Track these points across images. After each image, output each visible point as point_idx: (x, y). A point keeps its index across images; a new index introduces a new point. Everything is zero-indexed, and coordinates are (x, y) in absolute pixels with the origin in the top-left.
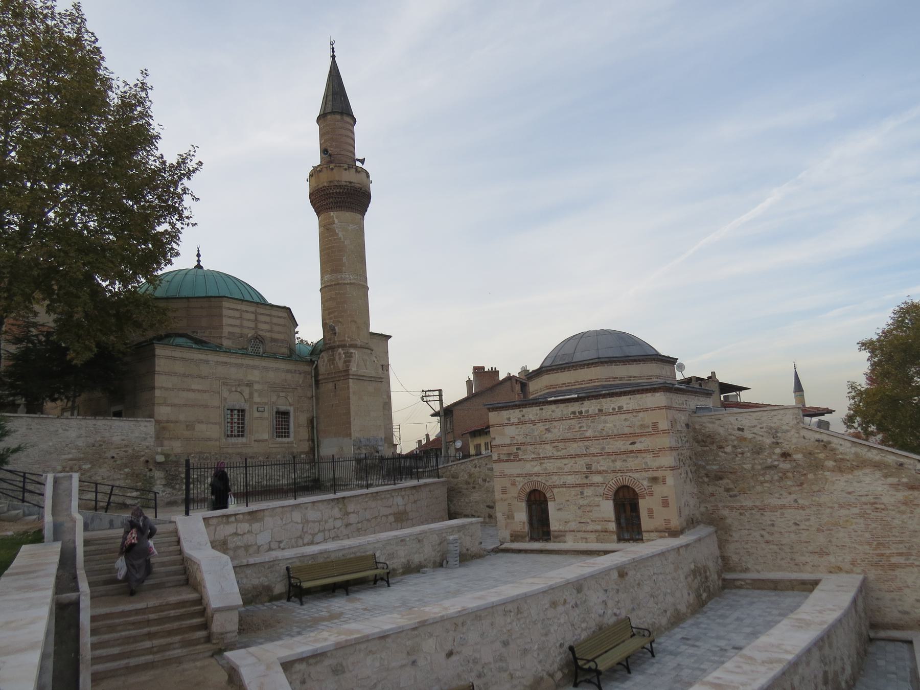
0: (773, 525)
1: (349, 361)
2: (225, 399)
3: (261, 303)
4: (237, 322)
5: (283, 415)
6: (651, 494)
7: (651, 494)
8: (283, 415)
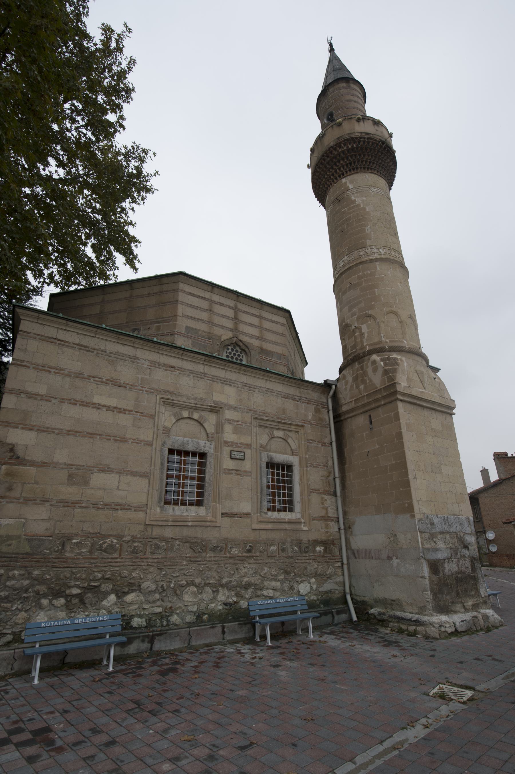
1: (395, 371)
2: (167, 431)
4: (205, 316)
5: (281, 471)
8: (281, 471)
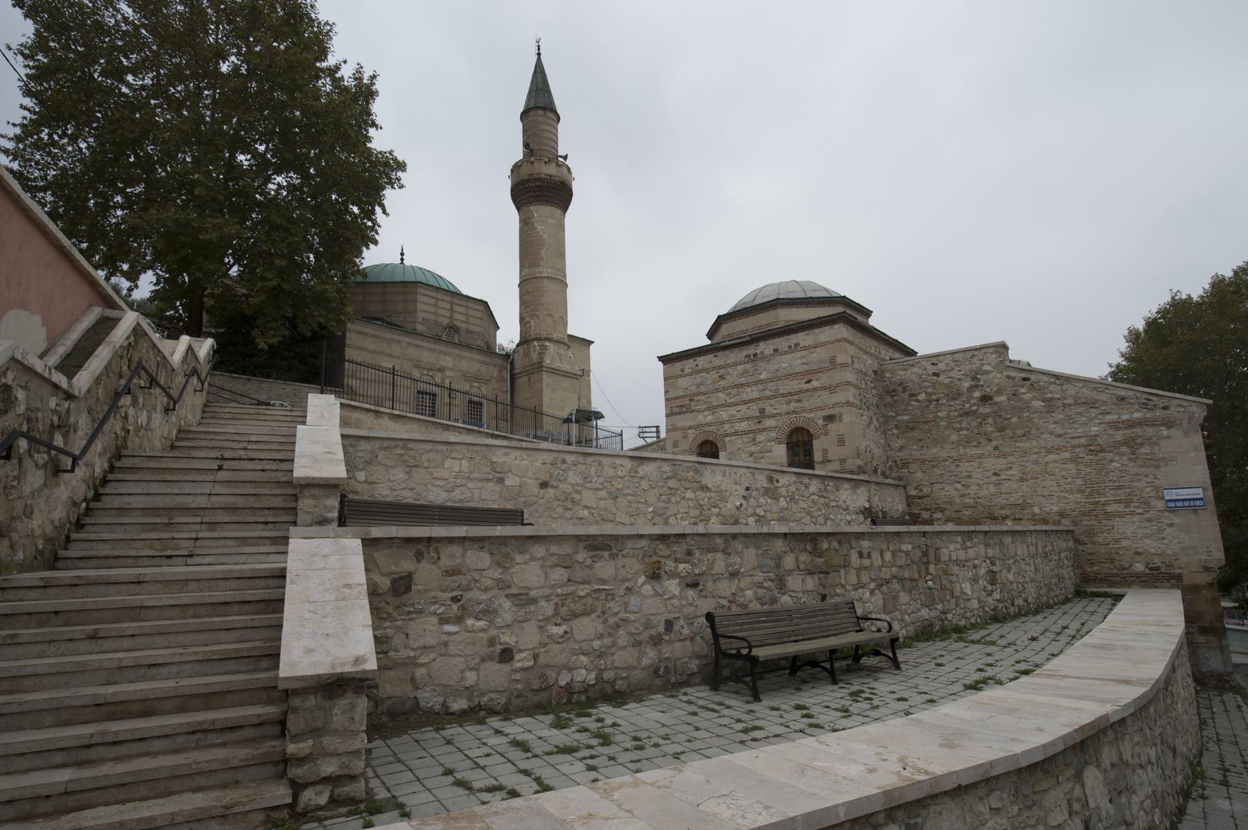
0: (969, 477)
3: (456, 295)
4: (432, 309)
6: (826, 434)
7: (826, 434)
